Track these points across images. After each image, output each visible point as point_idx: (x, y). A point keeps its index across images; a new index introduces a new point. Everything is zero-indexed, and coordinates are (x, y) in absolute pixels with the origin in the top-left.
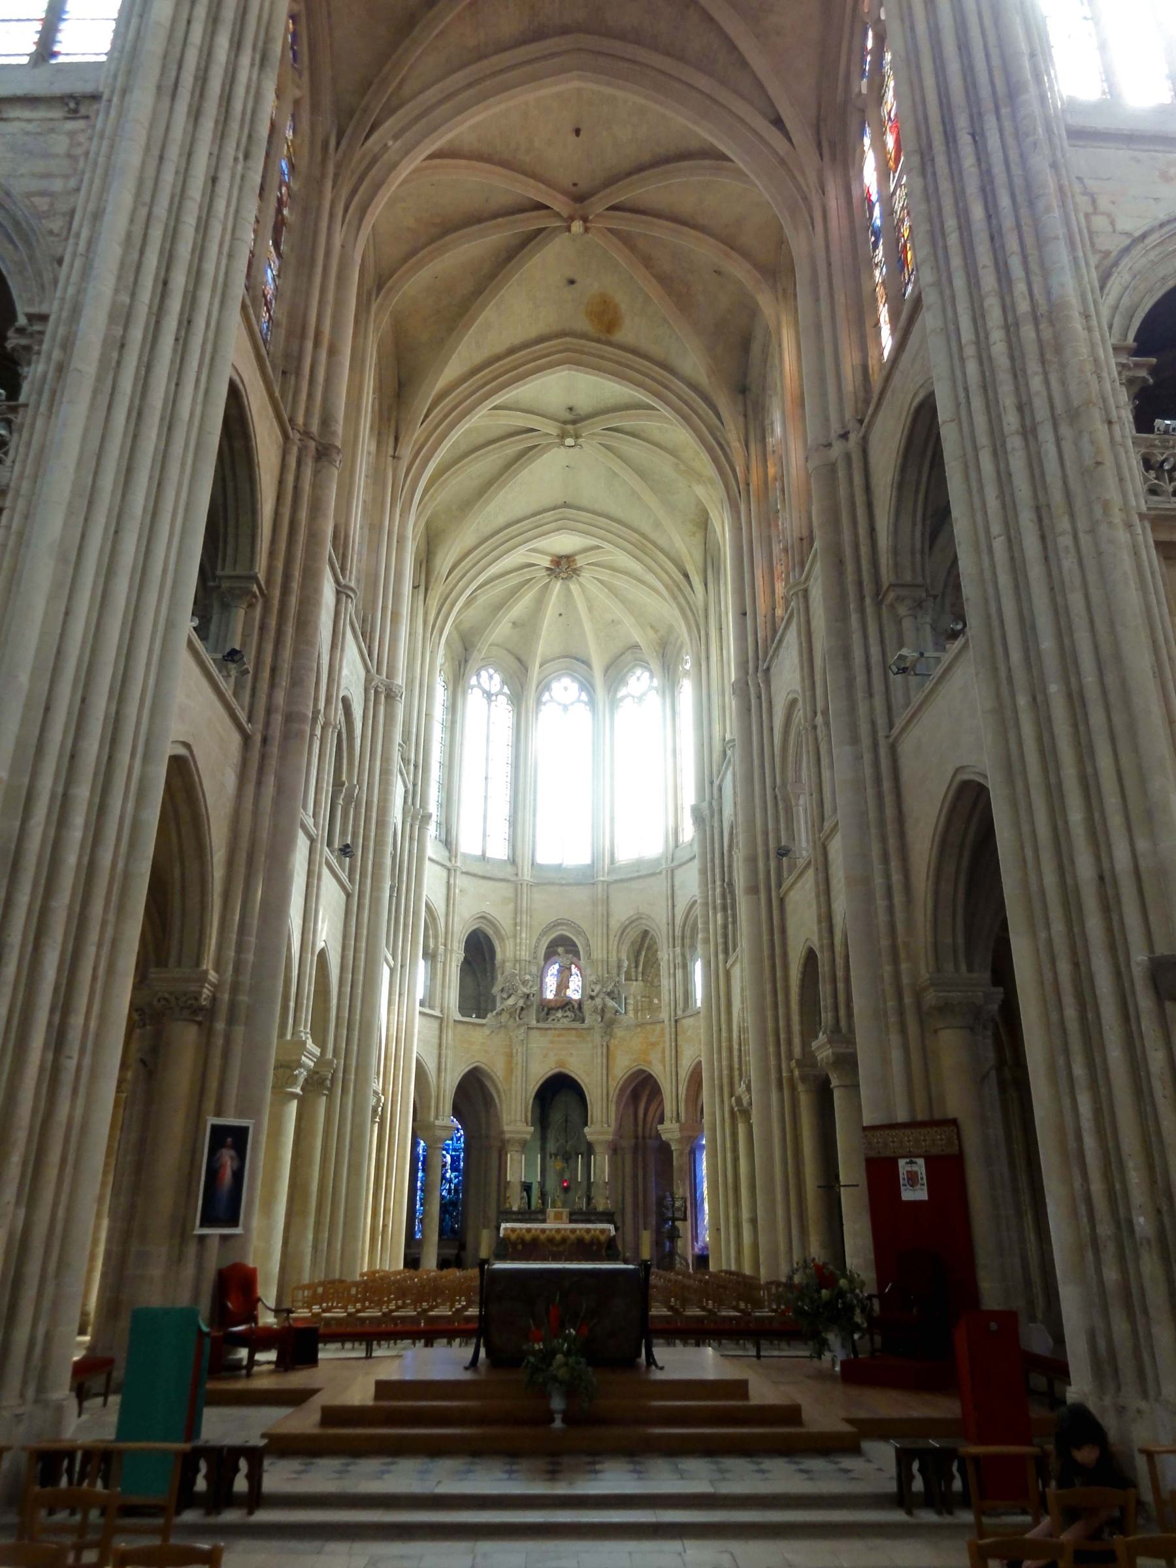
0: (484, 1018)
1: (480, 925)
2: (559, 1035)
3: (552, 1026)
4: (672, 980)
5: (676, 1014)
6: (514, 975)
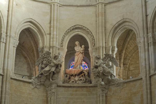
0: (31, 79)
1: (29, 26)
2: (76, 91)
3: (72, 85)
4: (146, 53)
5: (150, 73)
6: (48, 53)
